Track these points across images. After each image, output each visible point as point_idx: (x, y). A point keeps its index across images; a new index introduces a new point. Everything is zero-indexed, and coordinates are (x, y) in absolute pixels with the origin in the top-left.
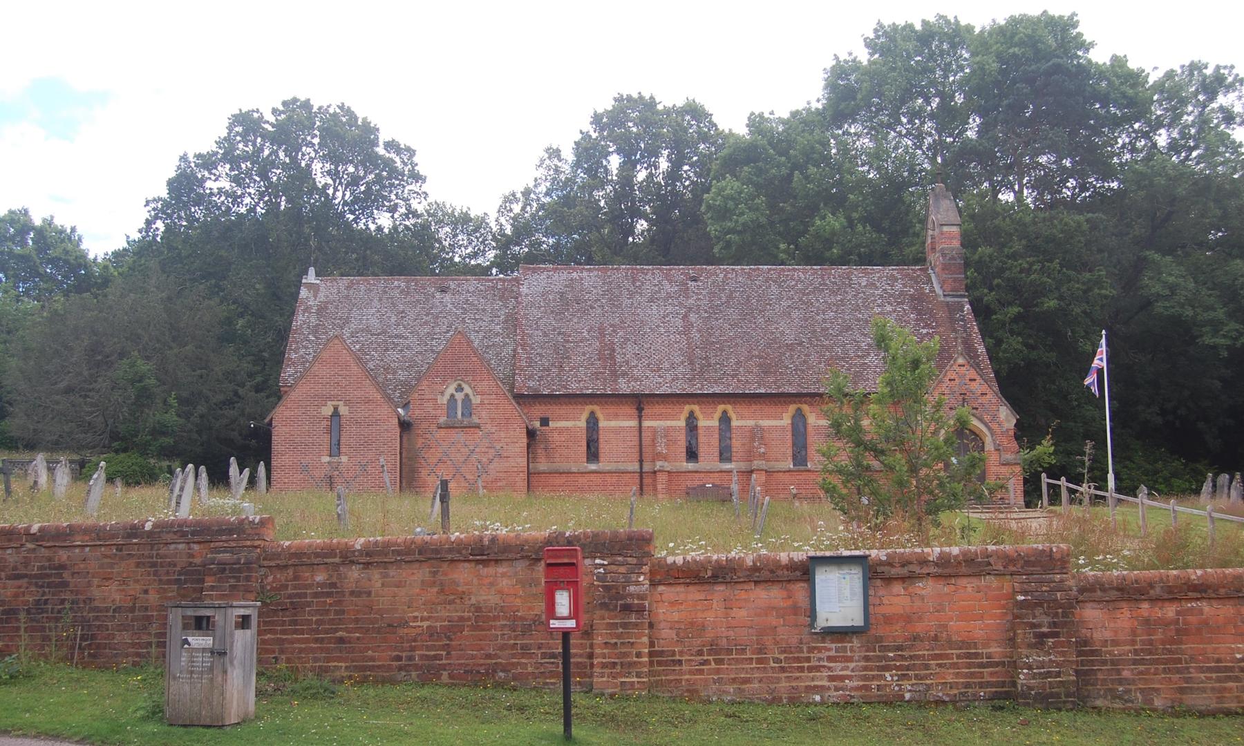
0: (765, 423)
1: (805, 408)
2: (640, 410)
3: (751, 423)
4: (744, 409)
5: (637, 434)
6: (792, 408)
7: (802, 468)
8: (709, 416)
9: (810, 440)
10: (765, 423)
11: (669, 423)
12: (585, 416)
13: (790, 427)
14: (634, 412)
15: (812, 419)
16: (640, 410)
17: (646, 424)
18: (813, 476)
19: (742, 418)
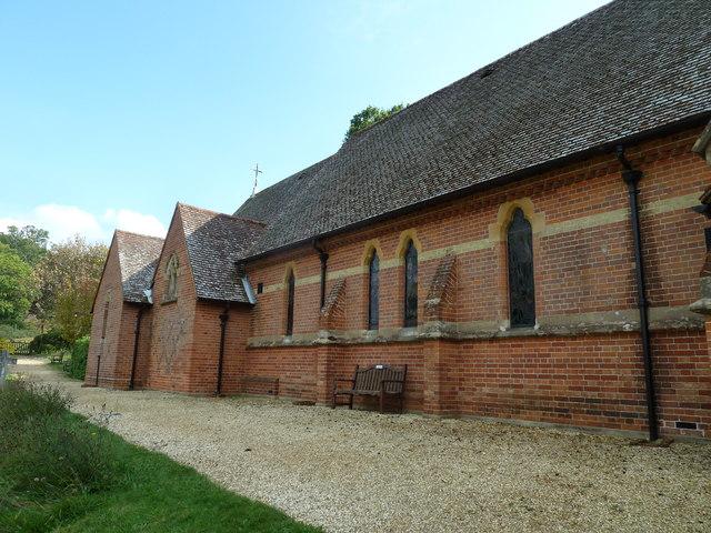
0: (461, 249)
1: (527, 204)
2: (324, 258)
3: (440, 253)
4: (432, 232)
5: (319, 292)
6: (503, 212)
7: (526, 331)
8: (389, 253)
9: (537, 269)
10: (461, 249)
11: (350, 272)
12: (284, 276)
13: (499, 251)
14: (318, 262)
15: (543, 226)
16: (324, 258)
17: (331, 276)
18: (544, 347)
19: (429, 246)
